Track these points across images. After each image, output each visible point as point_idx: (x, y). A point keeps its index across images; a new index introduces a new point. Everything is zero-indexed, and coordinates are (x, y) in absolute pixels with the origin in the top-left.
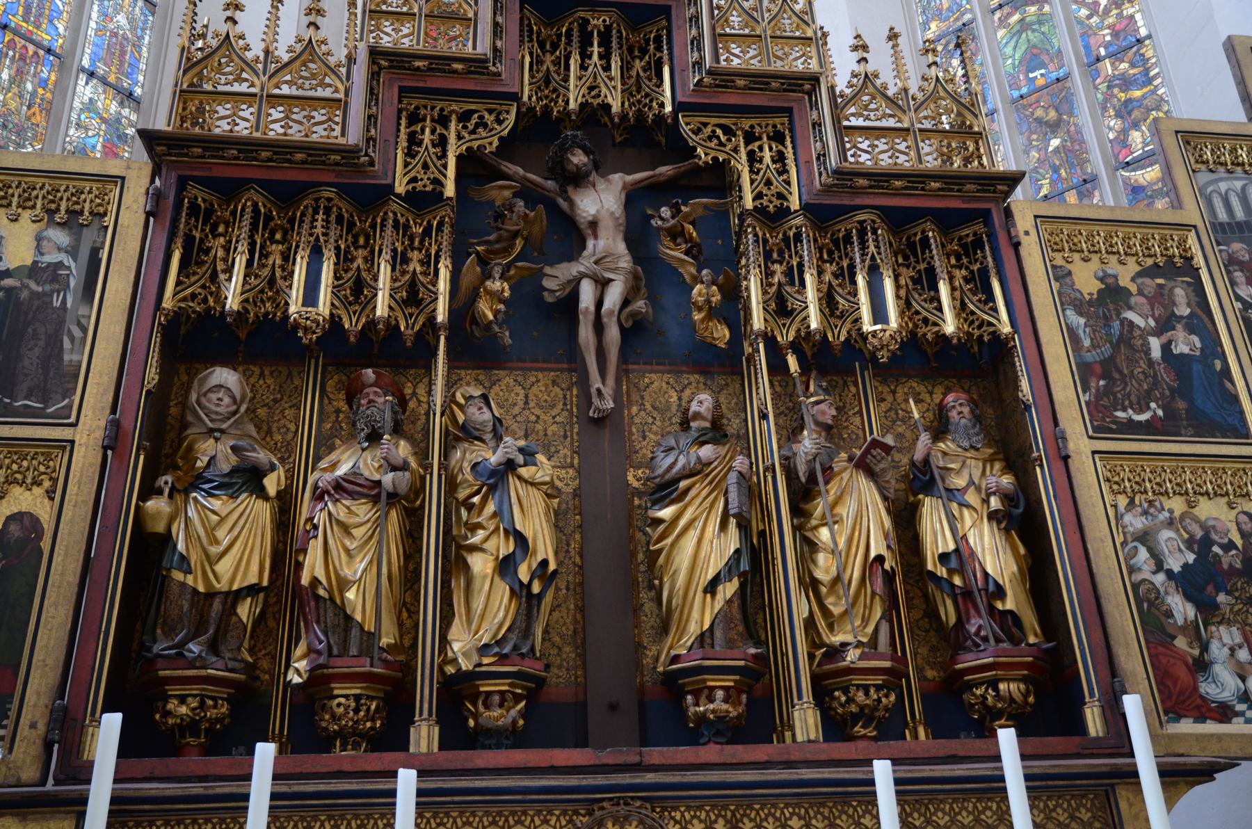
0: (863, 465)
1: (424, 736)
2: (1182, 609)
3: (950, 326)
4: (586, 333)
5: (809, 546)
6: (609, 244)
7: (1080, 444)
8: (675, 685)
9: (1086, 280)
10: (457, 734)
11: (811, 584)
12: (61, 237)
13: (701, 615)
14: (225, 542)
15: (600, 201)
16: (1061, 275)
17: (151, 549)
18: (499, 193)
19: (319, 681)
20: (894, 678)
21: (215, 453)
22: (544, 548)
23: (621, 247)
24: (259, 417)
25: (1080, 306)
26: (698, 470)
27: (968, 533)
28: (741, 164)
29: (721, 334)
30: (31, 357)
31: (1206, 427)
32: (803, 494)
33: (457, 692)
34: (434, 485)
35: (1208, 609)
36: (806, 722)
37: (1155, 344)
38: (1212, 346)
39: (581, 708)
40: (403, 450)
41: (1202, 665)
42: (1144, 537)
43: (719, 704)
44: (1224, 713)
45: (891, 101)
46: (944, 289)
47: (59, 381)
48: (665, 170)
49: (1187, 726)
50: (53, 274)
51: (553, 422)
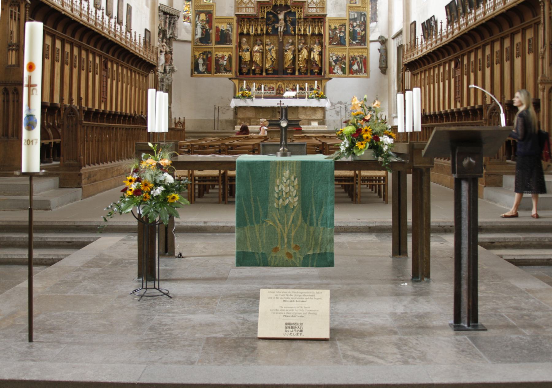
0: (306, 48)
1: (264, 74)
2: (333, 64)
3: (317, 33)
4: (279, 33)
5: (299, 57)
6: (282, 22)
7: (327, 47)
8: (287, 69)
9: (333, 27)
10: (267, 74)
11: (299, 61)
12: (228, 26)
13: (289, 63)
14: (247, 56)
15: (281, 17)
16: (330, 26)
17: (240, 57)
18: (271, 16)
19: (255, 69)
20: (307, 69)
21: (245, 47)
22: (275, 57)
23: (283, 22)
24: (248, 42)
25: (331, 30)
26: (289, 49)
27: (315, 55)
28: (297, 12)
29: (293, 33)
30: (228, 39)
31: (341, 44)
32: (299, 51)
33: (267, 70)
34: (265, 51)
35: (336, 64)
36: (297, 73)
37: (338, 35)
38: (345, 35)
39: (278, 71)
40: (261, 46)
41: (334, 69)
42: (332, 57)
43: (289, 72)
44: (335, 73)
45: (314, 3)
46: (317, 28)
47: (231, 41)
48: (289, 10)
49: (331, 75)
50: (228, 30)
51: (276, 42)
